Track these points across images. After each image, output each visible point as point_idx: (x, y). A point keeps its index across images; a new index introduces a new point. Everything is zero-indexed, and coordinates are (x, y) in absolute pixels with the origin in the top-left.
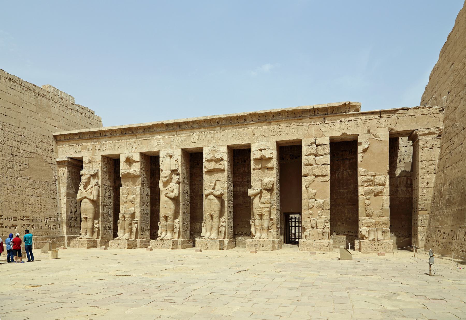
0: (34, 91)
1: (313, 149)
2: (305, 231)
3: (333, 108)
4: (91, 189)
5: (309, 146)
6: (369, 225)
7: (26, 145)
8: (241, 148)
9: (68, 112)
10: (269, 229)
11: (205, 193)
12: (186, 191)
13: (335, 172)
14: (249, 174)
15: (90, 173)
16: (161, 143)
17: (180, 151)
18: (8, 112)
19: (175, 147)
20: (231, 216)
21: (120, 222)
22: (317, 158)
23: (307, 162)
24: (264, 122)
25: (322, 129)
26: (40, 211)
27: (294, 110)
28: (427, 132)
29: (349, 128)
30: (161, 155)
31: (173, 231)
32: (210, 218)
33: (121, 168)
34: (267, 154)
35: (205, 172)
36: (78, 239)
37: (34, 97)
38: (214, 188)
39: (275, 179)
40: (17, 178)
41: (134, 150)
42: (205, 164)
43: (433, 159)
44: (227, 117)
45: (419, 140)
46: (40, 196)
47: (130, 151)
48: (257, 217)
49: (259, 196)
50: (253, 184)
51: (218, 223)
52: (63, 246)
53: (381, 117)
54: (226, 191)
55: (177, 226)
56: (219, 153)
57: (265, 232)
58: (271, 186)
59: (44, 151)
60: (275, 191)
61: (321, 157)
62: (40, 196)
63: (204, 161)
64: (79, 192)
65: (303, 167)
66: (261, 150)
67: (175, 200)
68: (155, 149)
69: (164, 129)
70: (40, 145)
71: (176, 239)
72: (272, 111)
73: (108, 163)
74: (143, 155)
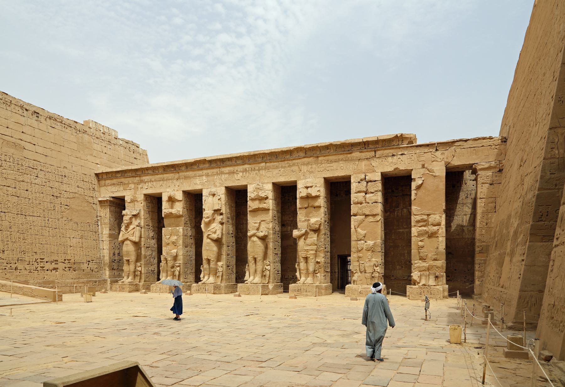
0: (75, 128)
2: (353, 276)
3: (384, 141)
4: (133, 231)
5: (359, 182)
6: (422, 269)
7: (67, 186)
10: (315, 272)
11: (249, 234)
14: (295, 214)
16: (204, 181)
17: (224, 189)
18: (48, 152)
19: (218, 185)
20: (278, 259)
22: (367, 196)
23: (356, 200)
25: (373, 164)
26: (82, 253)
27: (342, 144)
28: (487, 165)
32: (253, 261)
33: (163, 208)
34: (313, 192)
35: (250, 211)
36: (120, 283)
38: (258, 229)
39: (323, 219)
40: (58, 220)
42: (249, 203)
44: (272, 152)
46: (81, 238)
47: (173, 190)
48: (302, 260)
49: (304, 237)
50: (299, 224)
51: (261, 267)
52: (103, 290)
53: (437, 150)
54: (271, 232)
55: (220, 269)
57: (311, 276)
58: (317, 226)
59: (86, 191)
60: (323, 232)
61: (372, 195)
62: (81, 238)
64: (121, 233)
66: (307, 188)
67: (218, 241)
68: (198, 187)
70: (81, 184)
71: (219, 283)
73: (151, 202)
74: (187, 194)
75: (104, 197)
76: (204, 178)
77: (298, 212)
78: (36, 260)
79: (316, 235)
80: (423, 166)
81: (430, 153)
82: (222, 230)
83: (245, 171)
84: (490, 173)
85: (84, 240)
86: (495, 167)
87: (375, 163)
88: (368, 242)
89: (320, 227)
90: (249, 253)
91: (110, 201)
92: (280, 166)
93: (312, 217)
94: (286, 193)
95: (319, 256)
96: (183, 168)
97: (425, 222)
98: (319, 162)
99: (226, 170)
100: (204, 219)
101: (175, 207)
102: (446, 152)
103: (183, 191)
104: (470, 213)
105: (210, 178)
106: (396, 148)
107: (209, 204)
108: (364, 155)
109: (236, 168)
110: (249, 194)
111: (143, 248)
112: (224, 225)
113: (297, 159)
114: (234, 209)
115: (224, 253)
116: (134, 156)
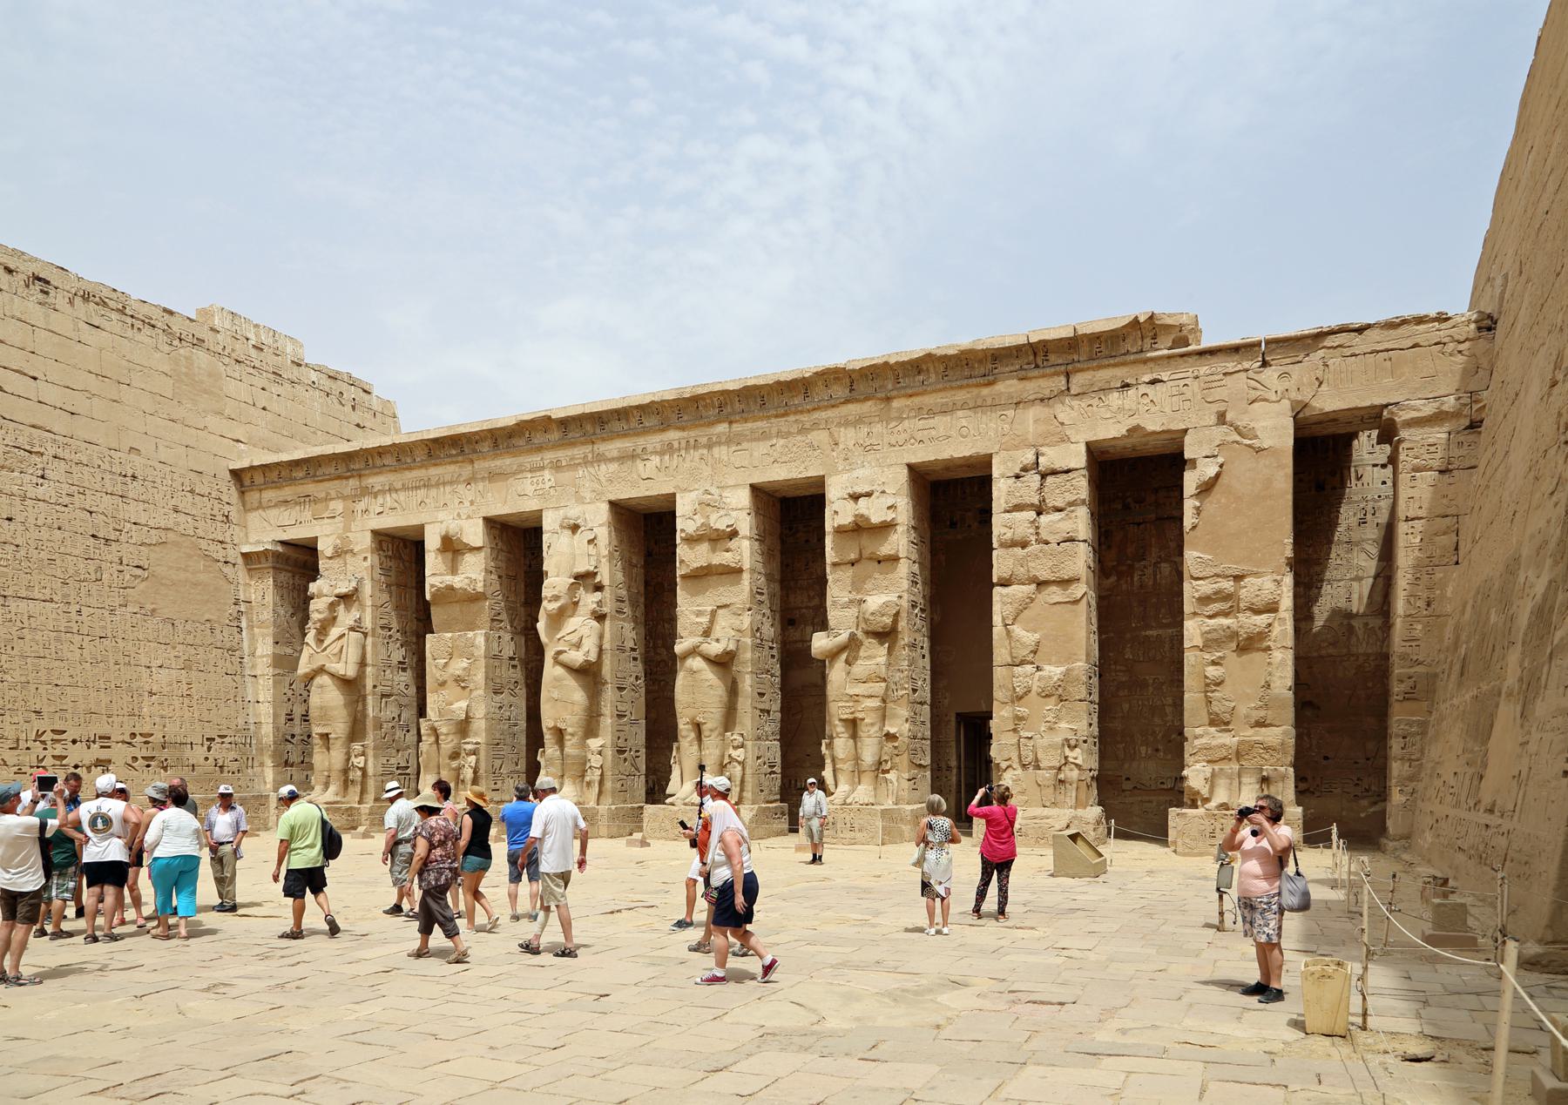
0: (167, 330)
6: (1218, 756)
7: (142, 506)
9: (280, 390)
10: (879, 767)
11: (679, 648)
13: (1131, 567)
14: (820, 584)
15: (337, 591)
16: (548, 484)
17: (605, 507)
18: (79, 403)
20: (772, 726)
22: (1044, 519)
23: (1009, 535)
24: (867, 399)
25: (1061, 417)
27: (963, 352)
28: (1428, 409)
29: (1153, 409)
30: (549, 523)
31: (583, 776)
32: (693, 735)
33: (427, 573)
34: (875, 511)
35: (683, 577)
37: (167, 348)
38: (707, 633)
39: (905, 596)
41: (466, 509)
42: (682, 551)
43: (1449, 511)
45: (1400, 441)
47: (454, 514)
48: (840, 728)
49: (844, 656)
50: (833, 615)
51: (717, 752)
53: (1265, 364)
54: (749, 641)
55: (595, 761)
56: (722, 512)
57: (867, 778)
58: (888, 620)
59: (201, 524)
60: (905, 638)
61: (1058, 516)
62: (187, 667)
63: (678, 541)
64: (306, 652)
65: (995, 553)
66: (855, 497)
67: (588, 674)
68: (529, 505)
69: (555, 435)
70: (185, 502)
71: (592, 804)
72: (892, 361)
73: (397, 556)
75: (258, 542)
76: (547, 474)
77: (830, 578)
78: (39, 735)
79: (883, 650)
80: (1221, 418)
81: (1243, 375)
82: (601, 637)
83: (669, 449)
84: (1439, 434)
85: (194, 673)
86: (1456, 415)
87: (1067, 411)
88: (1047, 667)
90: (679, 707)
91: (276, 555)
92: (774, 430)
93: (875, 595)
94: (792, 517)
95: (895, 716)
96: (485, 447)
97: (1227, 602)
98: (894, 414)
99: (613, 448)
100: (545, 603)
101: (461, 569)
103: (485, 519)
104: (1372, 572)
105: (566, 476)
106: (1134, 362)
107: (561, 558)
108: (1033, 387)
109: (641, 441)
110: (679, 524)
111: (370, 699)
112: (607, 622)
113: (826, 408)
114: (639, 572)
115: (607, 709)
116: (356, 417)
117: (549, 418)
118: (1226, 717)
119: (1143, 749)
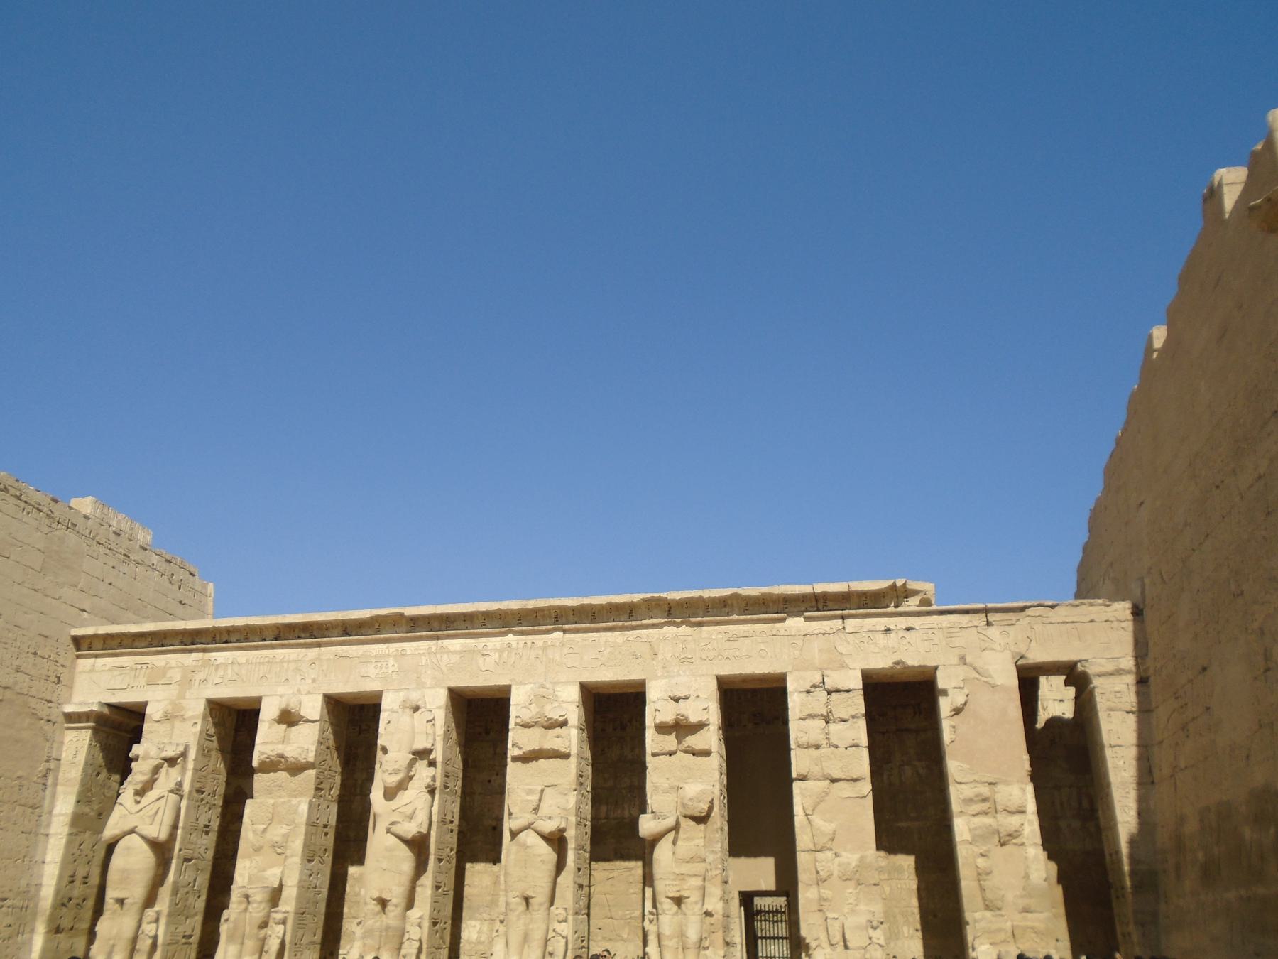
1: (818, 702)
5: (808, 692)
8: (617, 691)
11: (508, 825)
12: (449, 817)
14: (639, 768)
15: (164, 754)
16: (391, 669)
19: (429, 682)
21: (232, 919)
22: (832, 727)
33: (258, 740)
35: (515, 759)
38: (536, 810)
50: (653, 800)
54: (573, 819)
56: (556, 704)
58: (705, 807)
65: (793, 753)
67: (418, 845)
68: (370, 686)
88: (844, 854)
89: (711, 808)
102: (1011, 630)
103: (326, 696)
110: (513, 712)
111: (174, 862)
116: (179, 596)
117: (402, 615)
118: (999, 904)
119: (905, 929)
